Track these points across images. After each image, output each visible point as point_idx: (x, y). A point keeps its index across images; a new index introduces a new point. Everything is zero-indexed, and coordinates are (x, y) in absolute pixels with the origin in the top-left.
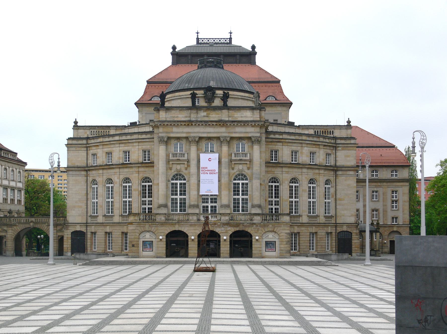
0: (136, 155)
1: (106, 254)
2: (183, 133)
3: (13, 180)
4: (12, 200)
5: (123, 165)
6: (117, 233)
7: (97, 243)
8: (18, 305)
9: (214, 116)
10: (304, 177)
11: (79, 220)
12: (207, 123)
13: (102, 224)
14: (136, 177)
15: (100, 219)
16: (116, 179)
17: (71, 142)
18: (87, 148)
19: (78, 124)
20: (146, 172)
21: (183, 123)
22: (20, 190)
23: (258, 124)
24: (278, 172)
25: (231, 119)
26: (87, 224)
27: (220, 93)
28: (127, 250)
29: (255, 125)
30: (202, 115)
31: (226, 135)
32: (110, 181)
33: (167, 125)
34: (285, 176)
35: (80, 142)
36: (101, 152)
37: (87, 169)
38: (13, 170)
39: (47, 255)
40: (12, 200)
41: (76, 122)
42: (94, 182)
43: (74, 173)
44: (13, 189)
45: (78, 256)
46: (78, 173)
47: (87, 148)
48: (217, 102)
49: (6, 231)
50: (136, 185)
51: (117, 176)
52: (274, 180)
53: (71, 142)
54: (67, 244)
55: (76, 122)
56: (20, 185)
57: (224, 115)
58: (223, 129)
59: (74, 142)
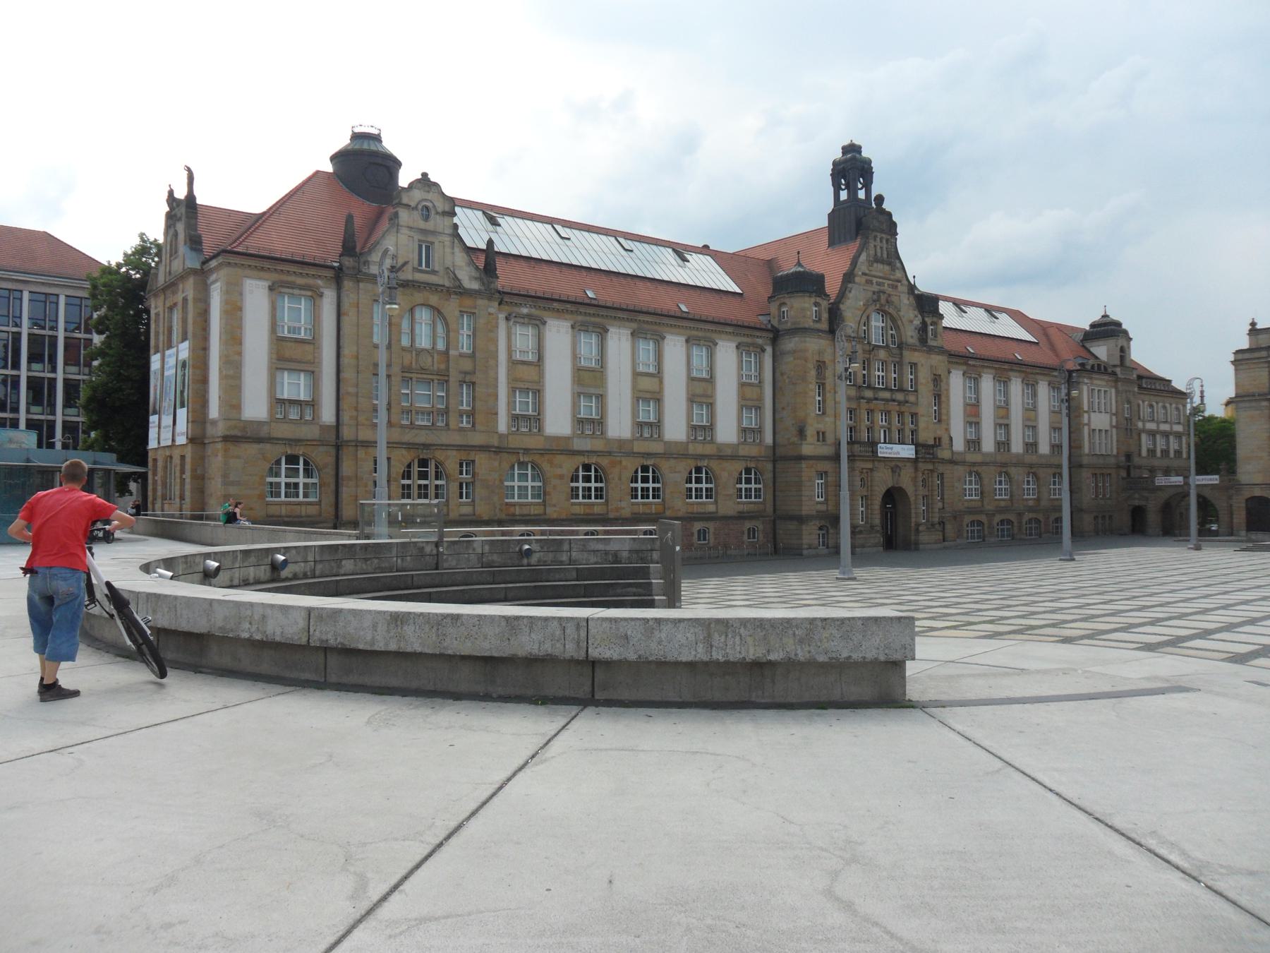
3: (1166, 422)
4: (1165, 452)
8: (1226, 607)
11: (1258, 479)
17: (1240, 356)
19: (1258, 327)
22: (1178, 436)
35: (1256, 355)
38: (1164, 407)
39: (1188, 535)
40: (1165, 452)
41: (1253, 324)
43: (1247, 405)
44: (1166, 435)
45: (1253, 537)
46: (1254, 404)
49: (1147, 499)
53: (1240, 356)
54: (1240, 517)
55: (1253, 324)
56: (1179, 428)
59: (1247, 356)
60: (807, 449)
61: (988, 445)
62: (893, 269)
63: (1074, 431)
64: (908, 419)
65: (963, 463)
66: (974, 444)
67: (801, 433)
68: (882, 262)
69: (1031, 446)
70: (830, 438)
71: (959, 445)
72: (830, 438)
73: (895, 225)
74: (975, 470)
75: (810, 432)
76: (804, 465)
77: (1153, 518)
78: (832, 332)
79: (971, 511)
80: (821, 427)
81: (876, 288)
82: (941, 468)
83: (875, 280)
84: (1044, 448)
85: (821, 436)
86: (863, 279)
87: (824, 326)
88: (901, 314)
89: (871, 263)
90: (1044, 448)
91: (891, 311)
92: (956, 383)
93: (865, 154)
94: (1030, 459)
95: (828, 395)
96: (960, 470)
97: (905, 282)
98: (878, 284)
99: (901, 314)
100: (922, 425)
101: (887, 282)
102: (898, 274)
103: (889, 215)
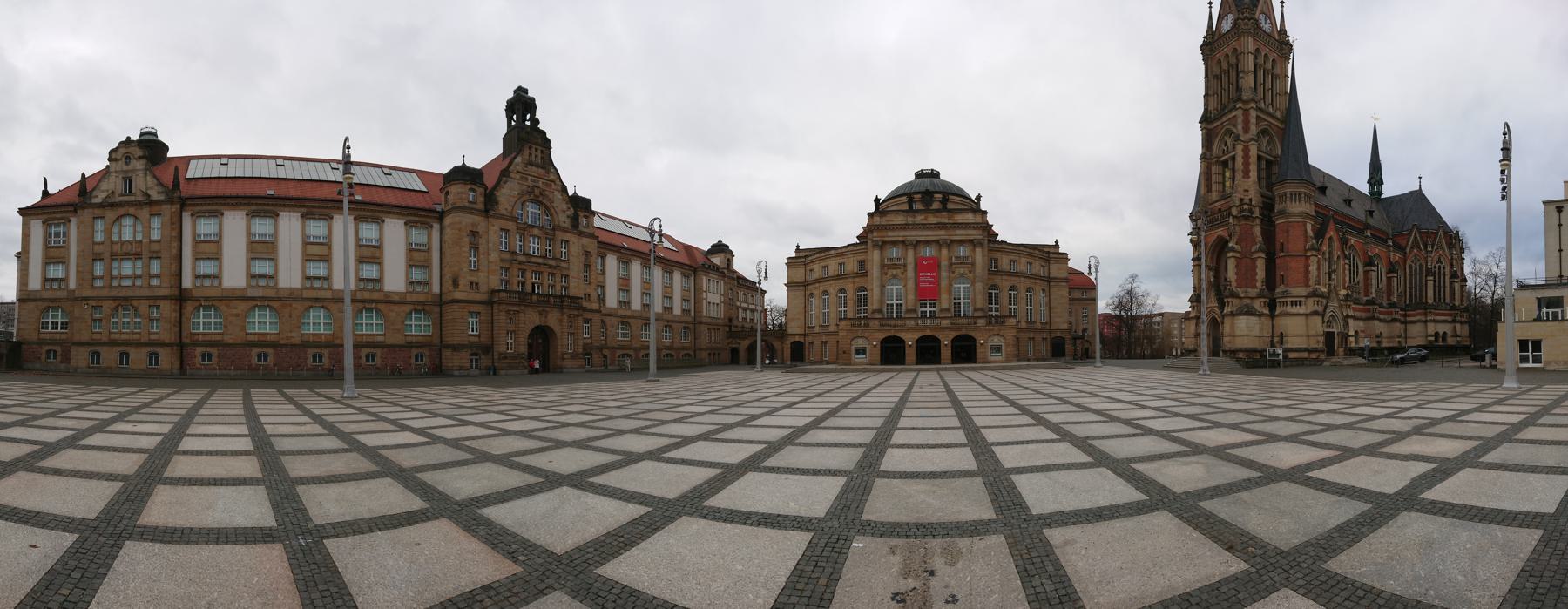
0: (851, 265)
1: (821, 362)
5: (838, 277)
6: (832, 341)
7: (813, 353)
10: (1023, 284)
11: (798, 331)
13: (819, 334)
14: (850, 287)
15: (817, 330)
16: (831, 290)
18: (805, 265)
20: (860, 282)
24: (997, 280)
26: (805, 335)
28: (840, 360)
32: (826, 292)
34: (1005, 283)
36: (817, 267)
37: (805, 284)
42: (812, 295)
47: (805, 265)
50: (851, 294)
51: (832, 288)
52: (994, 287)
54: (787, 353)
61: (636, 305)
63: (698, 301)
64: (558, 278)
65: (616, 315)
66: (626, 304)
67: (455, 283)
69: (668, 309)
70: (483, 288)
71: (612, 301)
72: (483, 288)
74: (625, 321)
75: (463, 282)
77: (743, 354)
79: (622, 348)
80: (475, 279)
82: (589, 316)
84: (677, 311)
85: (474, 285)
90: (677, 311)
92: (612, 261)
94: (666, 317)
96: (614, 320)
100: (573, 283)
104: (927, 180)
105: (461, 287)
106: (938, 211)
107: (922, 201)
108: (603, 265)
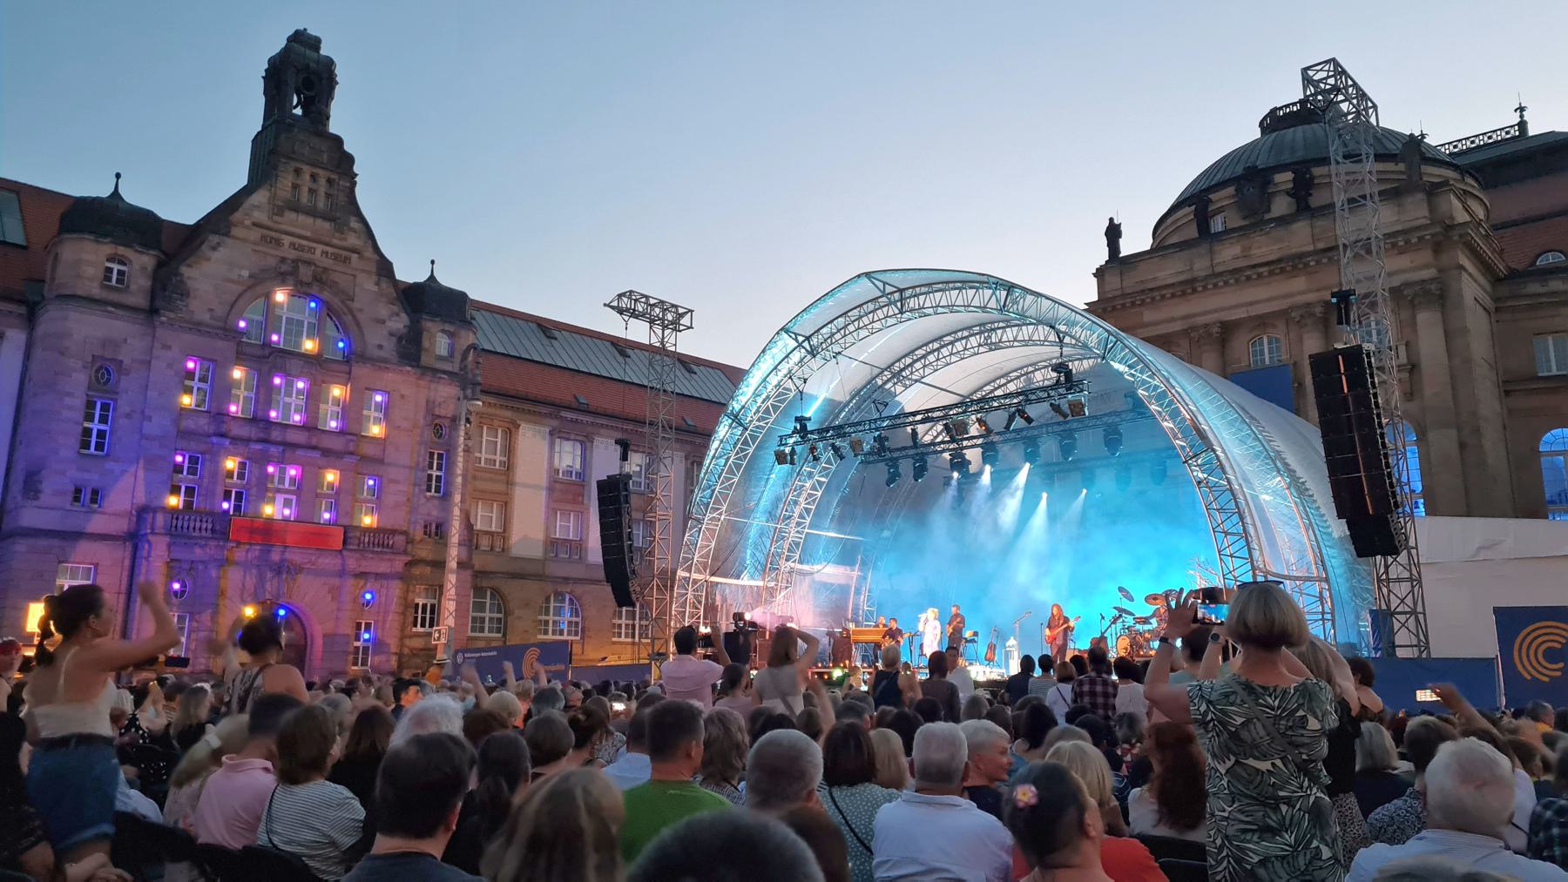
2: (1173, 320)
9: (1265, 248)
12: (1238, 276)
21: (1167, 292)
23: (1421, 239)
25: (1321, 245)
27: (1284, 178)
29: (1407, 242)
30: (1229, 254)
31: (1311, 297)
33: (1123, 305)
48: (1281, 206)
57: (1300, 236)
58: (1299, 283)
60: (30, 516)
62: (340, 227)
67: (31, 486)
68: (312, 212)
73: (350, 159)
76: (21, 546)
78: (152, 311)
81: (292, 254)
83: (287, 240)
86: (255, 234)
87: (139, 299)
88: (356, 305)
89: (278, 210)
91: (326, 295)
93: (323, 52)
95: (122, 422)
97: (369, 253)
98: (292, 245)
99: (356, 305)
101: (320, 248)
102: (353, 240)
103: (338, 141)
104: (1298, 133)
105: (46, 497)
106: (1283, 221)
107: (1242, 205)
108: (509, 450)
